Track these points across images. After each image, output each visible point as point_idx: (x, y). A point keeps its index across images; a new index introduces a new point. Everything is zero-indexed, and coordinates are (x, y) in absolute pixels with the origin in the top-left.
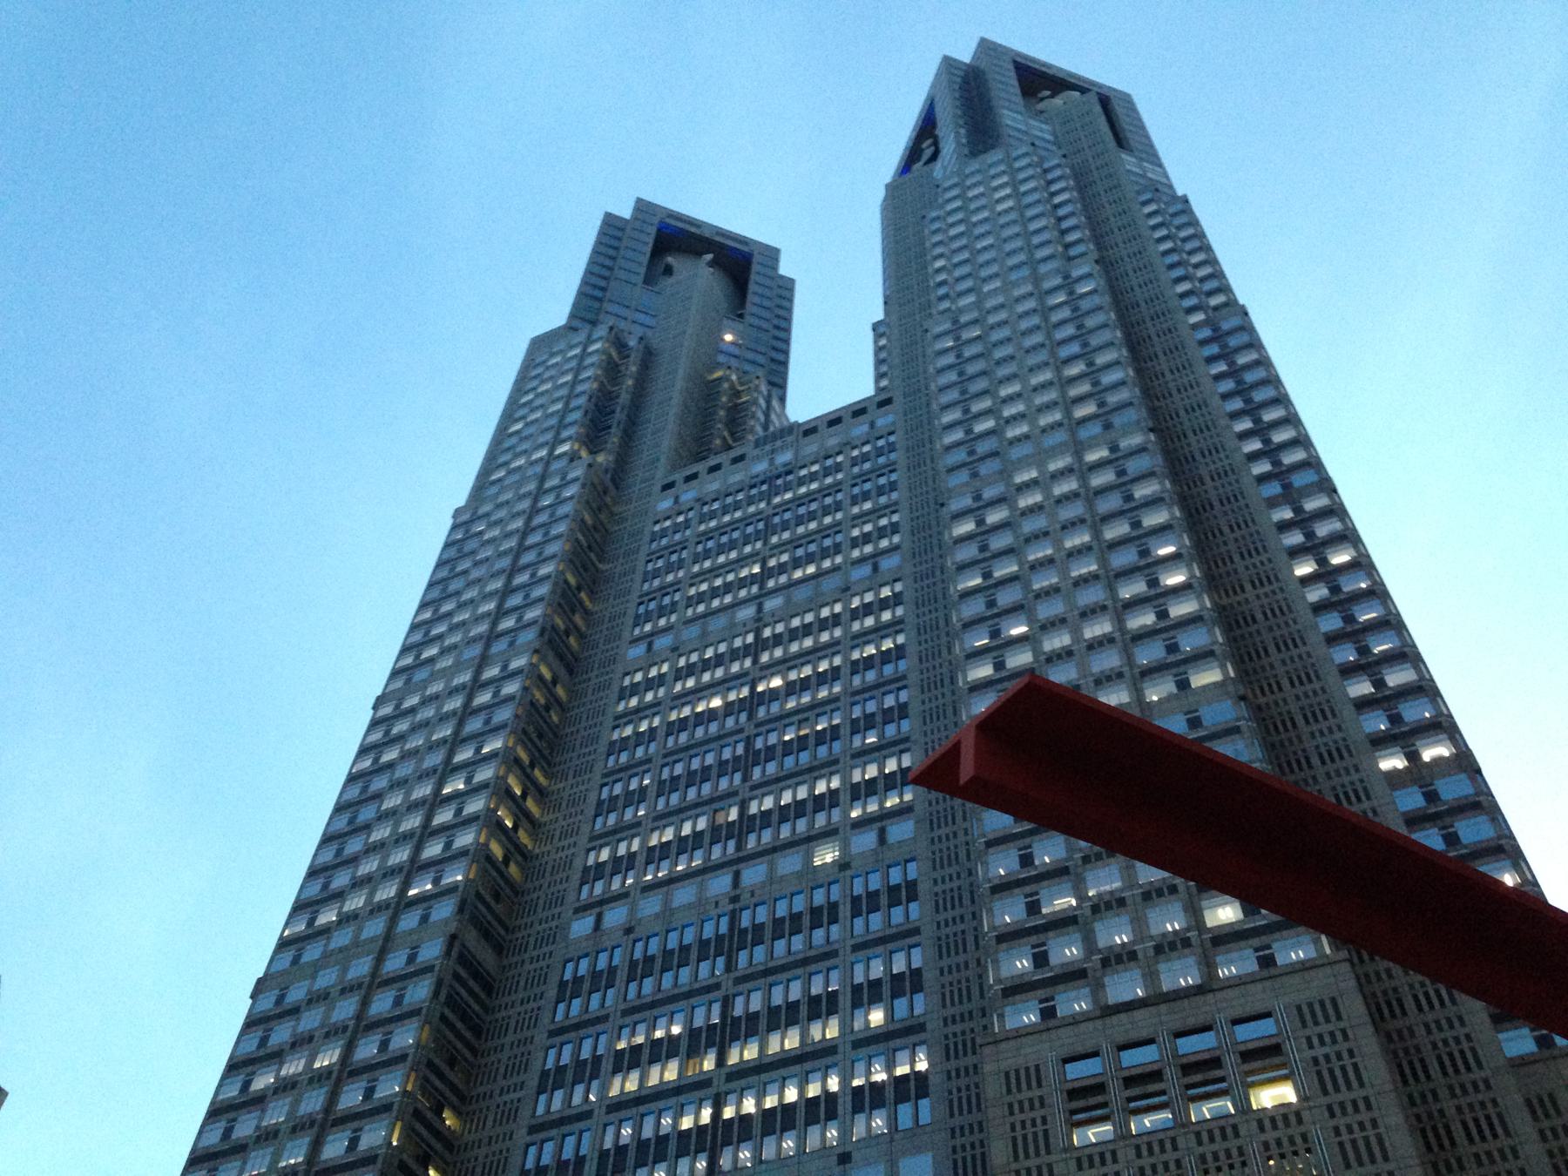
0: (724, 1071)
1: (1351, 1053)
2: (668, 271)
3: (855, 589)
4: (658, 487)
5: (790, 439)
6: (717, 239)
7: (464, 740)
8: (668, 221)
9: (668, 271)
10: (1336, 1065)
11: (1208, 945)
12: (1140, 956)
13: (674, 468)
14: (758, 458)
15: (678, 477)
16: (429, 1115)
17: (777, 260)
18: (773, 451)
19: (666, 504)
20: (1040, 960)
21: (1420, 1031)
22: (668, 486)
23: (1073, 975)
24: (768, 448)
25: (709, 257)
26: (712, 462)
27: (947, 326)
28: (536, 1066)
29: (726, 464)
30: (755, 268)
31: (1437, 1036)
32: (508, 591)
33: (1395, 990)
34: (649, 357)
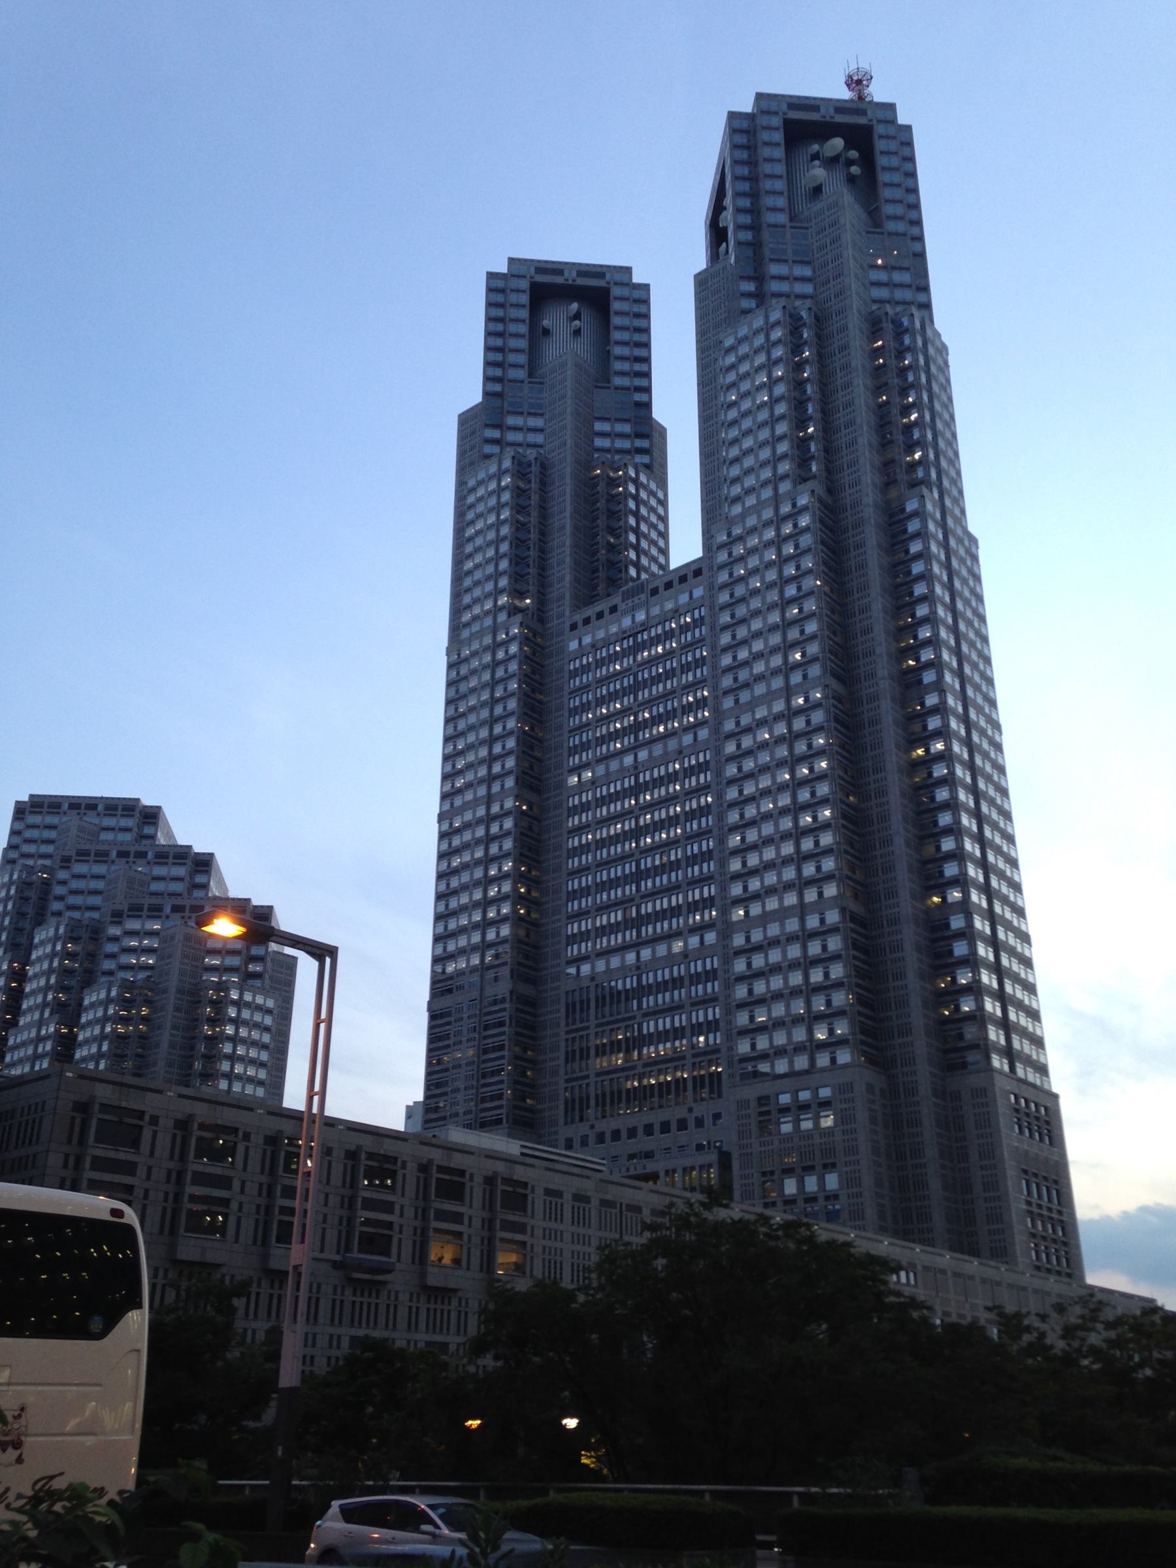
3: (685, 752)
4: (567, 625)
5: (643, 597)
6: (581, 281)
8: (541, 278)
9: (546, 332)
14: (624, 613)
15: (578, 618)
16: (521, 1079)
17: (631, 273)
18: (633, 609)
19: (573, 645)
22: (574, 627)
24: (629, 602)
25: (575, 306)
26: (598, 608)
29: (607, 612)
30: (616, 306)
34: (544, 467)
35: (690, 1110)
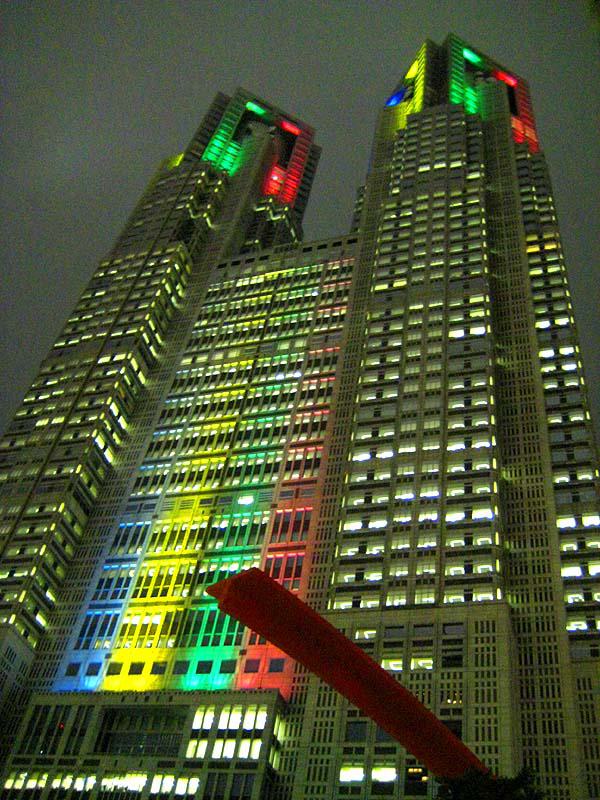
0: (192, 598)
1: (494, 649)
2: (249, 132)
4: (217, 264)
5: (295, 252)
7: (84, 396)
9: (249, 132)
10: (486, 653)
11: (443, 583)
12: (408, 583)
13: (226, 255)
15: (229, 261)
20: (359, 577)
21: (535, 639)
22: (220, 266)
23: (373, 588)
25: (273, 128)
27: (394, 205)
28: (99, 575)
31: (542, 645)
32: (121, 314)
33: (529, 619)
35: (243, 653)
